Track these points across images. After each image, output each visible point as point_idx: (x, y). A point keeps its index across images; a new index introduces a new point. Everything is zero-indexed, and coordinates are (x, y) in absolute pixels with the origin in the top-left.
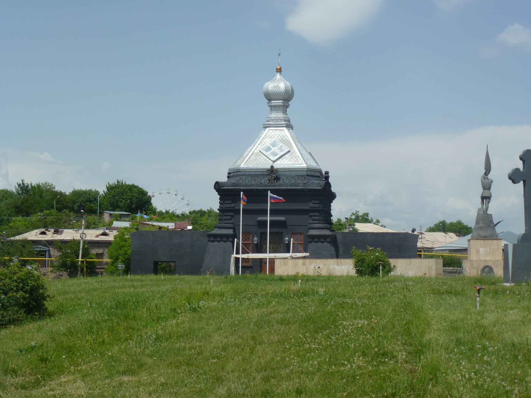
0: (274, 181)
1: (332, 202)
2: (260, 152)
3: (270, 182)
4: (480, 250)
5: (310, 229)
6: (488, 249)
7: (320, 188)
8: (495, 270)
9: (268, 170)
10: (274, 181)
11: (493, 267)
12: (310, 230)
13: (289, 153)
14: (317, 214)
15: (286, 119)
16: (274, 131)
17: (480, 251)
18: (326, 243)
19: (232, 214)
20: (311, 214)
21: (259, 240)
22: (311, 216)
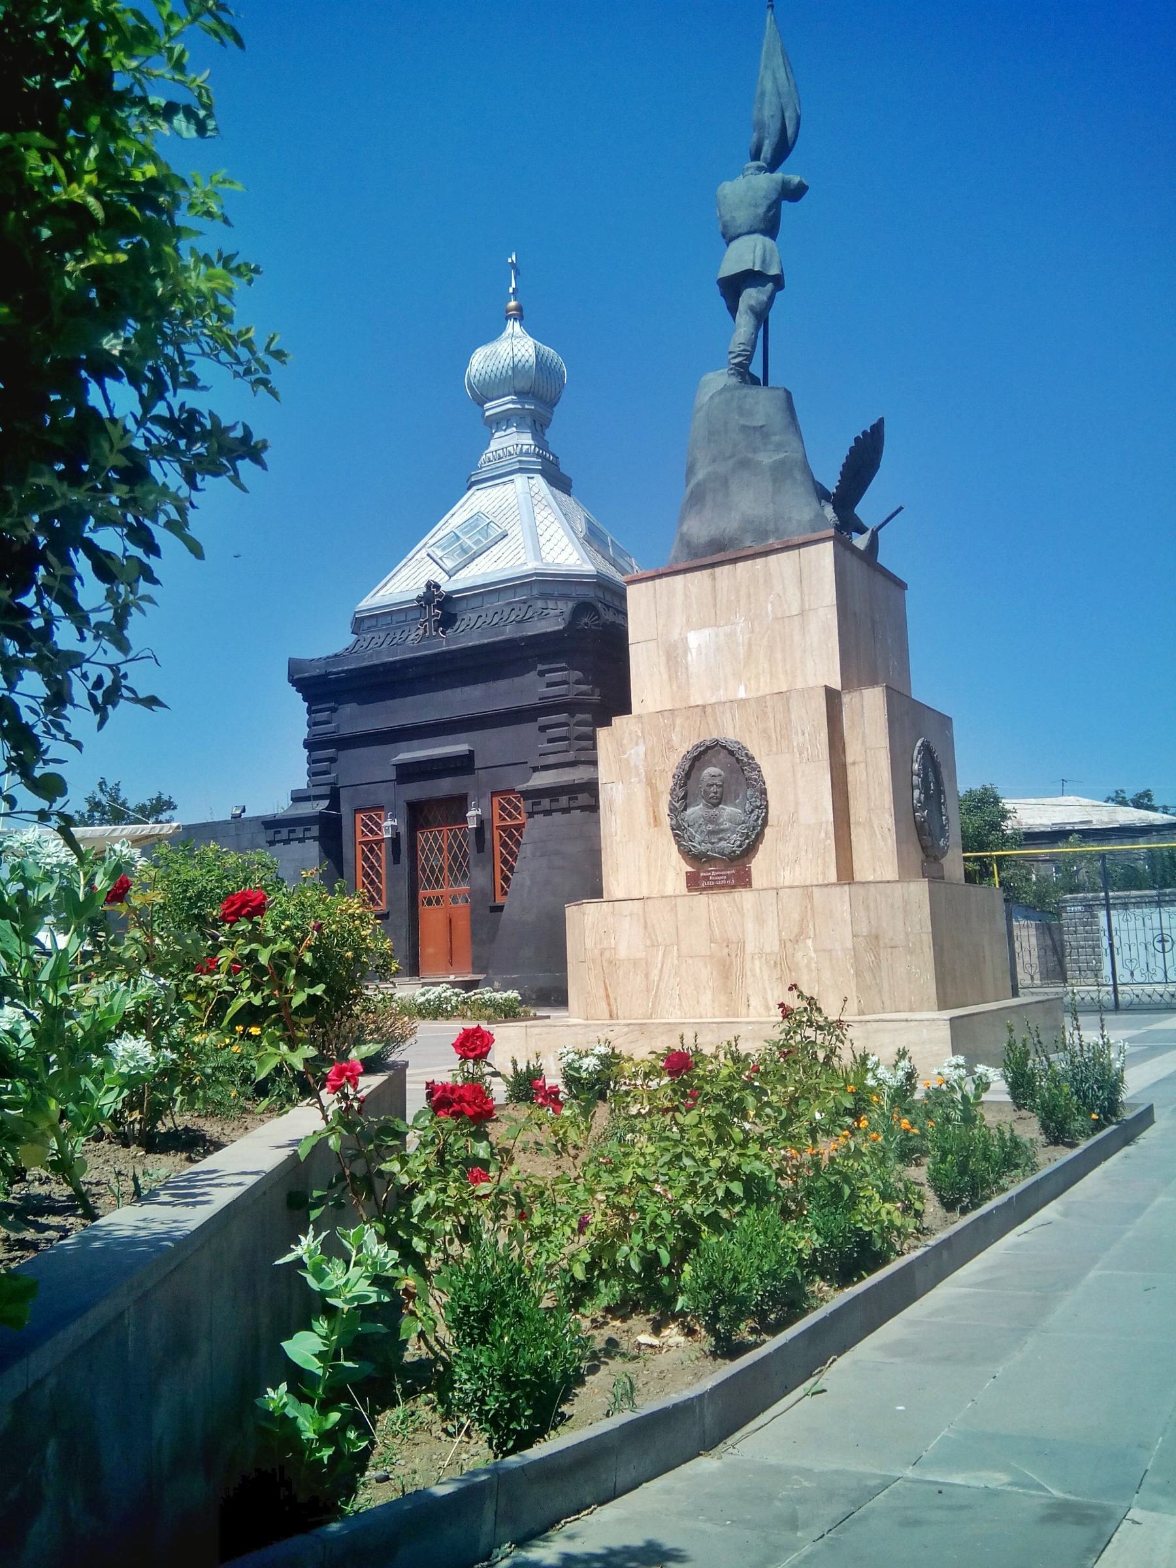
0: (436, 630)
2: (428, 555)
3: (427, 634)
4: (685, 640)
5: (535, 769)
6: (741, 623)
7: (561, 627)
8: (770, 769)
9: (419, 599)
10: (436, 630)
11: (756, 748)
12: (536, 775)
13: (506, 540)
14: (562, 717)
15: (525, 447)
16: (490, 490)
17: (686, 650)
18: (576, 813)
20: (543, 720)
21: (403, 830)
22: (543, 729)
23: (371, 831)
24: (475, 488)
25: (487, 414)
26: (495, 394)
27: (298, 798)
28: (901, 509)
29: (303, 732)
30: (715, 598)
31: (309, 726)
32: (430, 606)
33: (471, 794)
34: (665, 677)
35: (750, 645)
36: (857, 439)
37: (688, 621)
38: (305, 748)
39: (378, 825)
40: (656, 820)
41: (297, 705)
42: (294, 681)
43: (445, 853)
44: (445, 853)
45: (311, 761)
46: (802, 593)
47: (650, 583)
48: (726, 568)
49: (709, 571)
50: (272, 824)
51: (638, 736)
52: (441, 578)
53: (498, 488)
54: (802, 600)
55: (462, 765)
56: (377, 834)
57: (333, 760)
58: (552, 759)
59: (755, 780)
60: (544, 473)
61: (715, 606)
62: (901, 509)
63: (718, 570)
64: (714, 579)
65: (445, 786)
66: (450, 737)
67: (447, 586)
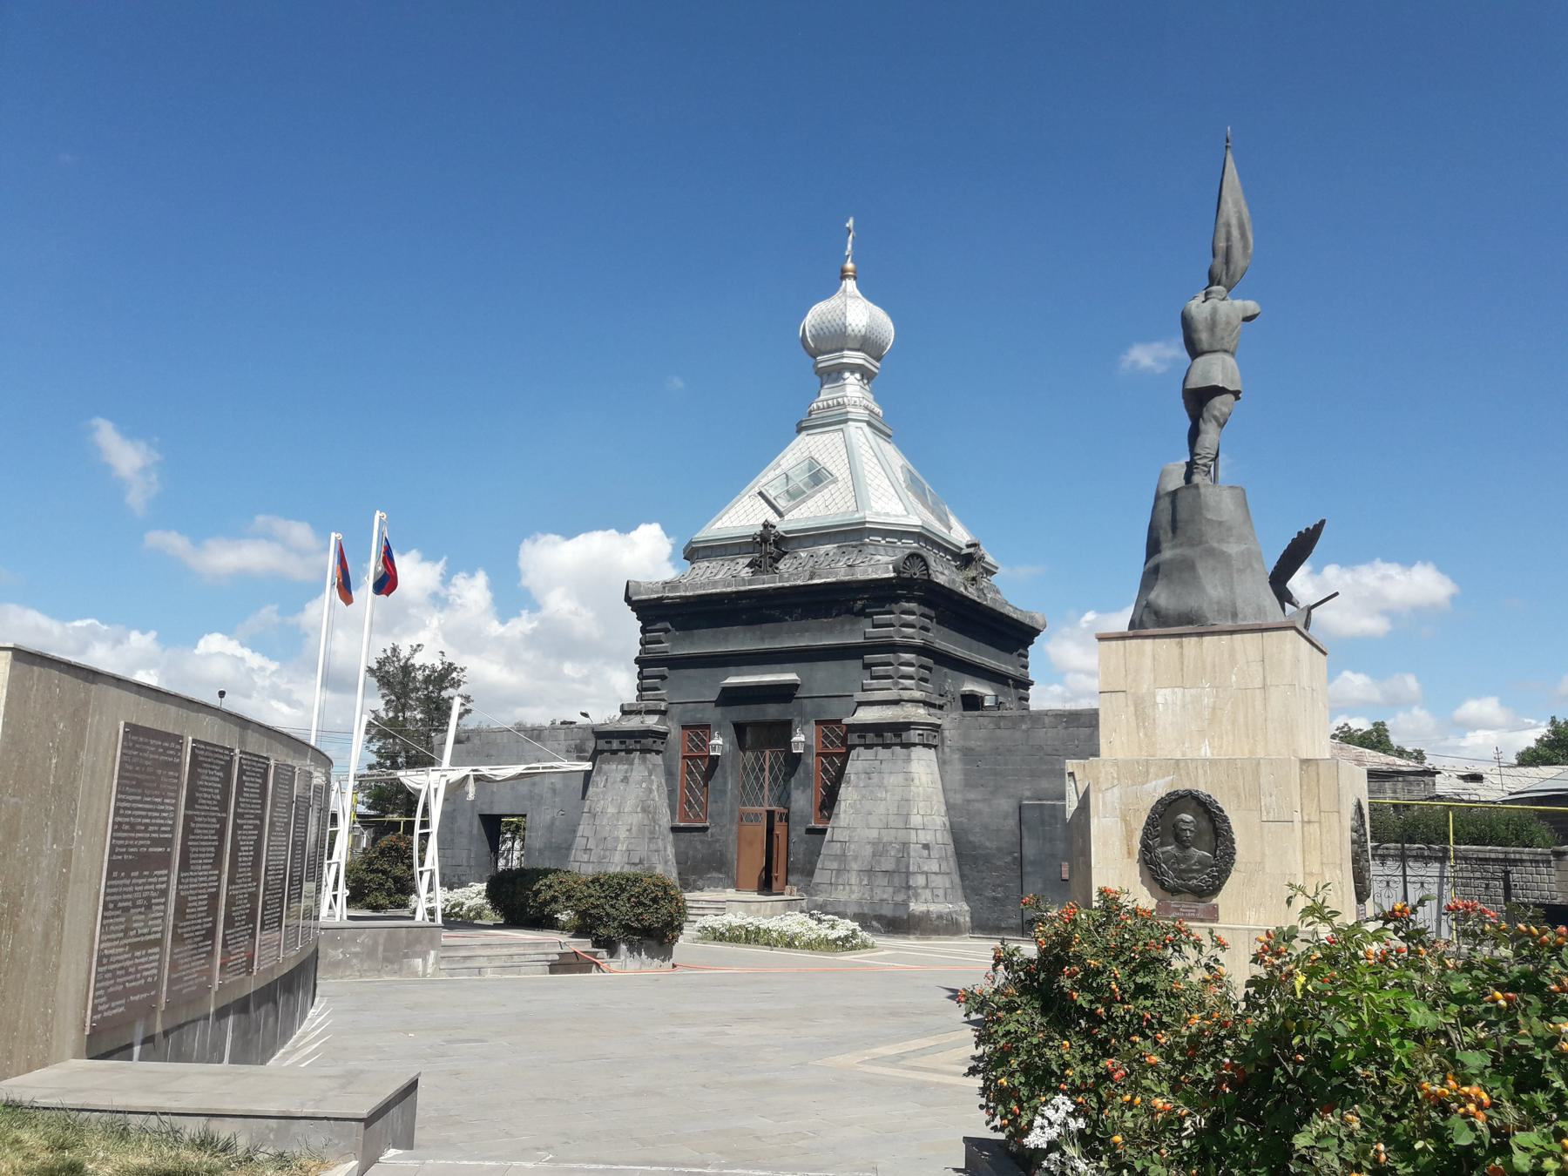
1: (1032, 643)
5: (860, 704)
16: (819, 437)
17: (1155, 704)
19: (664, 670)
20: (869, 658)
23: (697, 746)
24: (804, 433)
25: (820, 366)
26: (828, 348)
27: (626, 712)
28: (1337, 594)
29: (636, 649)
30: (1182, 663)
31: (641, 644)
32: (766, 543)
33: (796, 720)
34: (1134, 725)
35: (1214, 709)
36: (1300, 533)
37: (1155, 680)
38: (636, 663)
39: (702, 741)
40: (1129, 853)
41: (632, 625)
42: (628, 599)
43: (767, 773)
44: (767, 773)
45: (641, 676)
46: (1264, 669)
47: (1120, 642)
48: (1194, 640)
49: (1178, 640)
50: (602, 734)
51: (1113, 778)
52: (773, 518)
53: (827, 435)
54: (1264, 678)
55: (784, 693)
56: (702, 750)
57: (663, 678)
58: (878, 696)
59: (1226, 831)
60: (869, 424)
61: (1182, 670)
62: (1337, 594)
63: (1185, 640)
64: (1182, 647)
65: (772, 711)
66: (778, 667)
67: (782, 526)
